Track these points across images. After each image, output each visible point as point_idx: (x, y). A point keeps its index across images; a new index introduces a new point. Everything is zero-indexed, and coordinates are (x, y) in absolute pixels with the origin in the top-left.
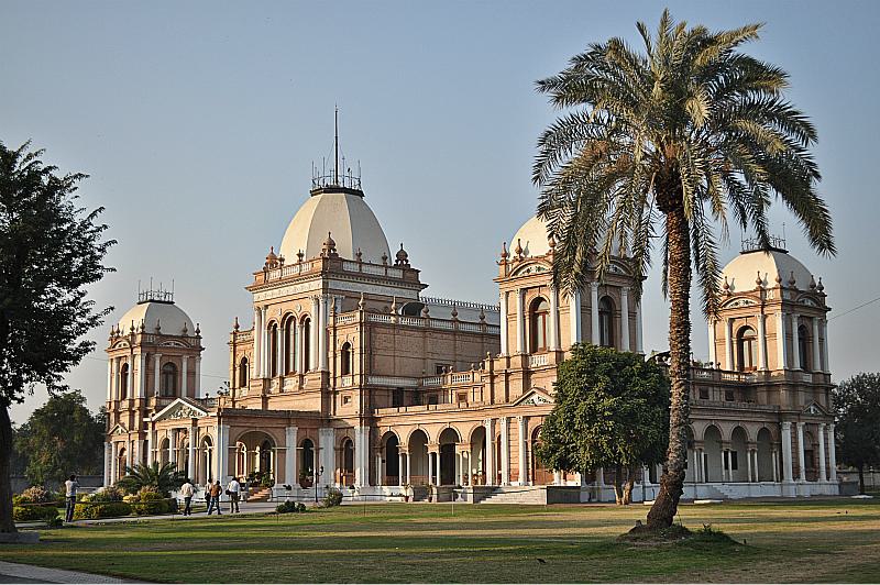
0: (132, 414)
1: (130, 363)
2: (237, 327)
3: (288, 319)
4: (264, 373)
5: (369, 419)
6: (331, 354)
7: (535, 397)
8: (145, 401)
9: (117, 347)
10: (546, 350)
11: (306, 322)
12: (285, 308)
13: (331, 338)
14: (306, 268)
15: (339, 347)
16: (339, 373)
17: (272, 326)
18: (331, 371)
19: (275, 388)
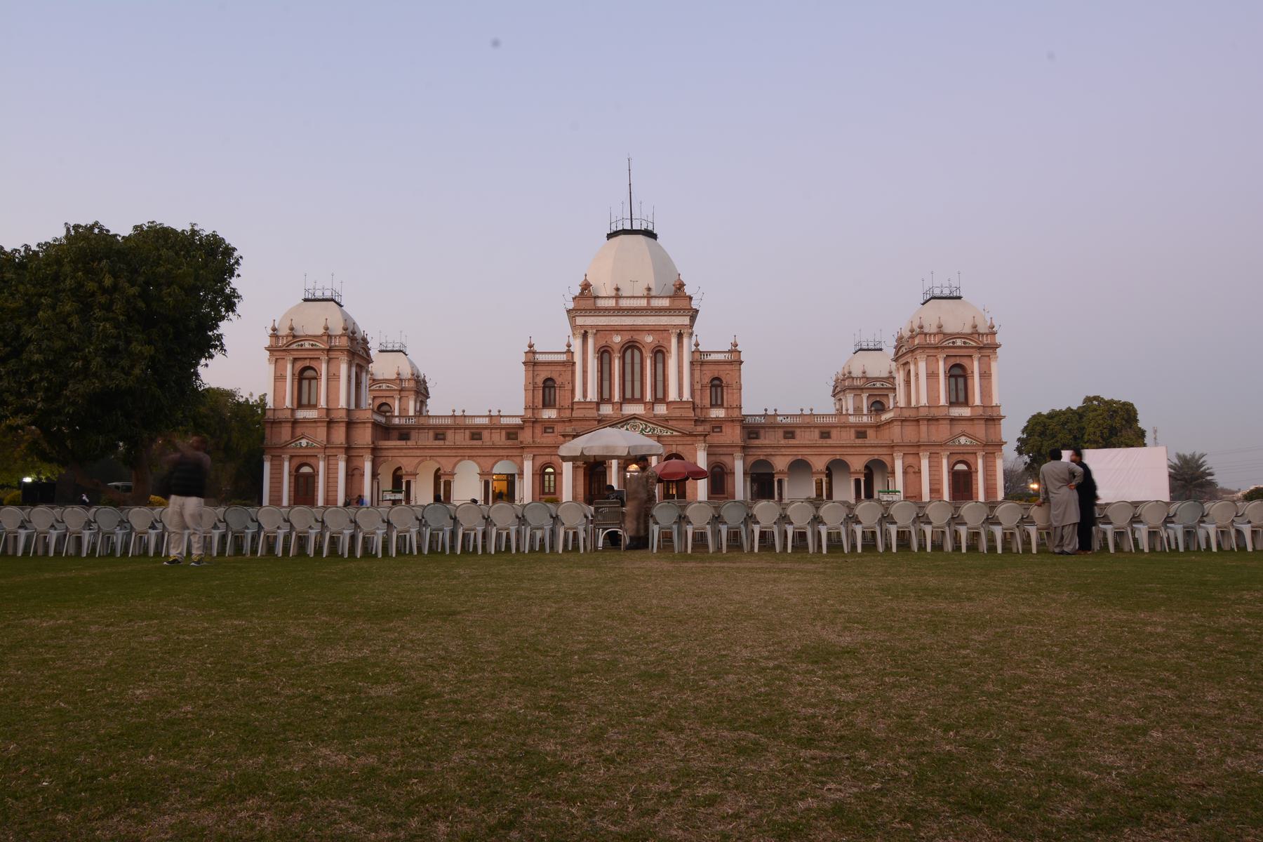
0: (330, 423)
1: (324, 368)
2: (531, 346)
3: (631, 346)
4: (592, 395)
5: (744, 448)
6: (698, 386)
7: (963, 440)
8: (348, 411)
9: (294, 346)
10: (966, 403)
11: (660, 353)
12: (627, 337)
13: (697, 373)
14: (665, 303)
15: (707, 380)
16: (707, 402)
17: (604, 353)
18: (698, 401)
19: (606, 410)
